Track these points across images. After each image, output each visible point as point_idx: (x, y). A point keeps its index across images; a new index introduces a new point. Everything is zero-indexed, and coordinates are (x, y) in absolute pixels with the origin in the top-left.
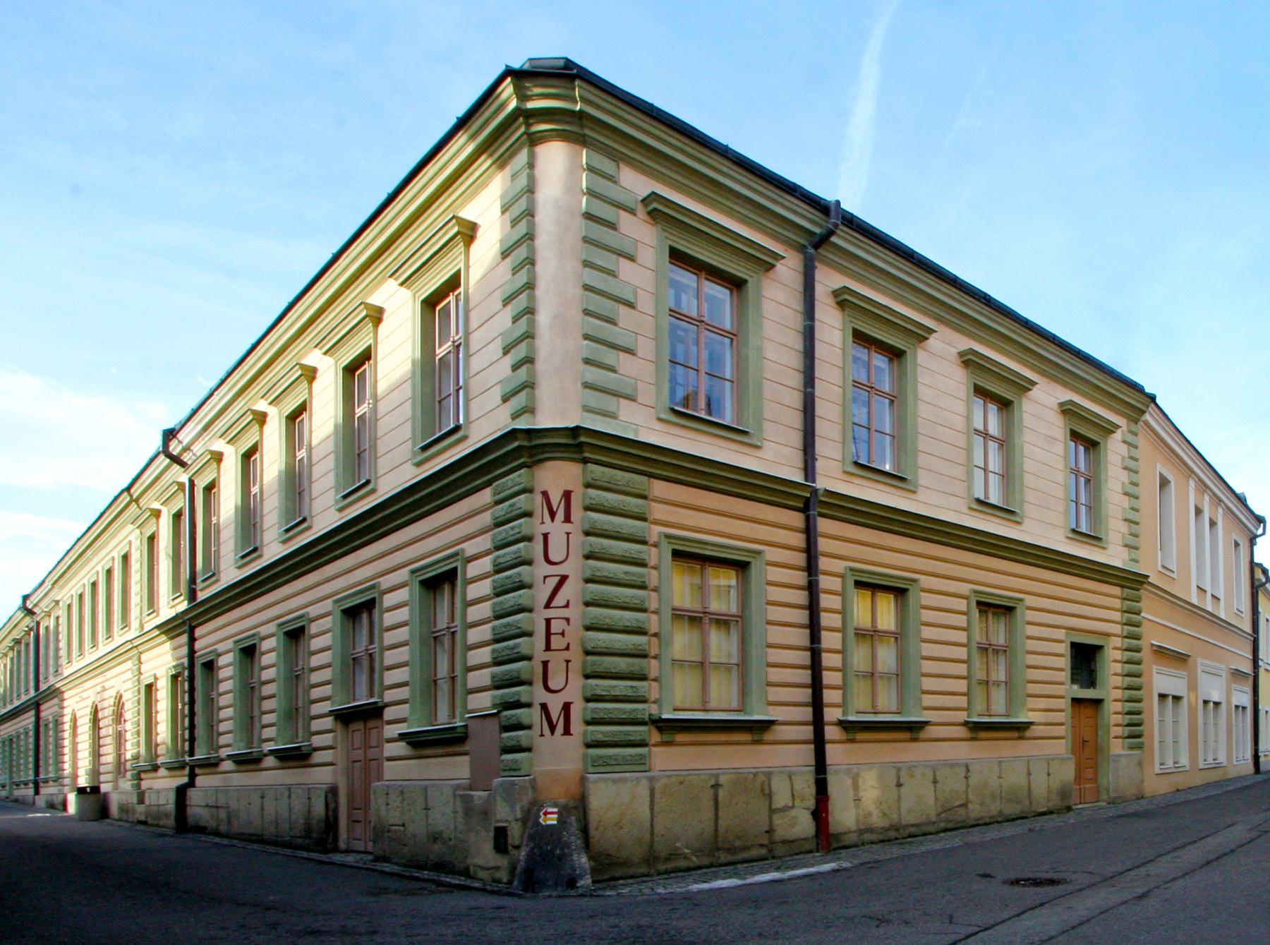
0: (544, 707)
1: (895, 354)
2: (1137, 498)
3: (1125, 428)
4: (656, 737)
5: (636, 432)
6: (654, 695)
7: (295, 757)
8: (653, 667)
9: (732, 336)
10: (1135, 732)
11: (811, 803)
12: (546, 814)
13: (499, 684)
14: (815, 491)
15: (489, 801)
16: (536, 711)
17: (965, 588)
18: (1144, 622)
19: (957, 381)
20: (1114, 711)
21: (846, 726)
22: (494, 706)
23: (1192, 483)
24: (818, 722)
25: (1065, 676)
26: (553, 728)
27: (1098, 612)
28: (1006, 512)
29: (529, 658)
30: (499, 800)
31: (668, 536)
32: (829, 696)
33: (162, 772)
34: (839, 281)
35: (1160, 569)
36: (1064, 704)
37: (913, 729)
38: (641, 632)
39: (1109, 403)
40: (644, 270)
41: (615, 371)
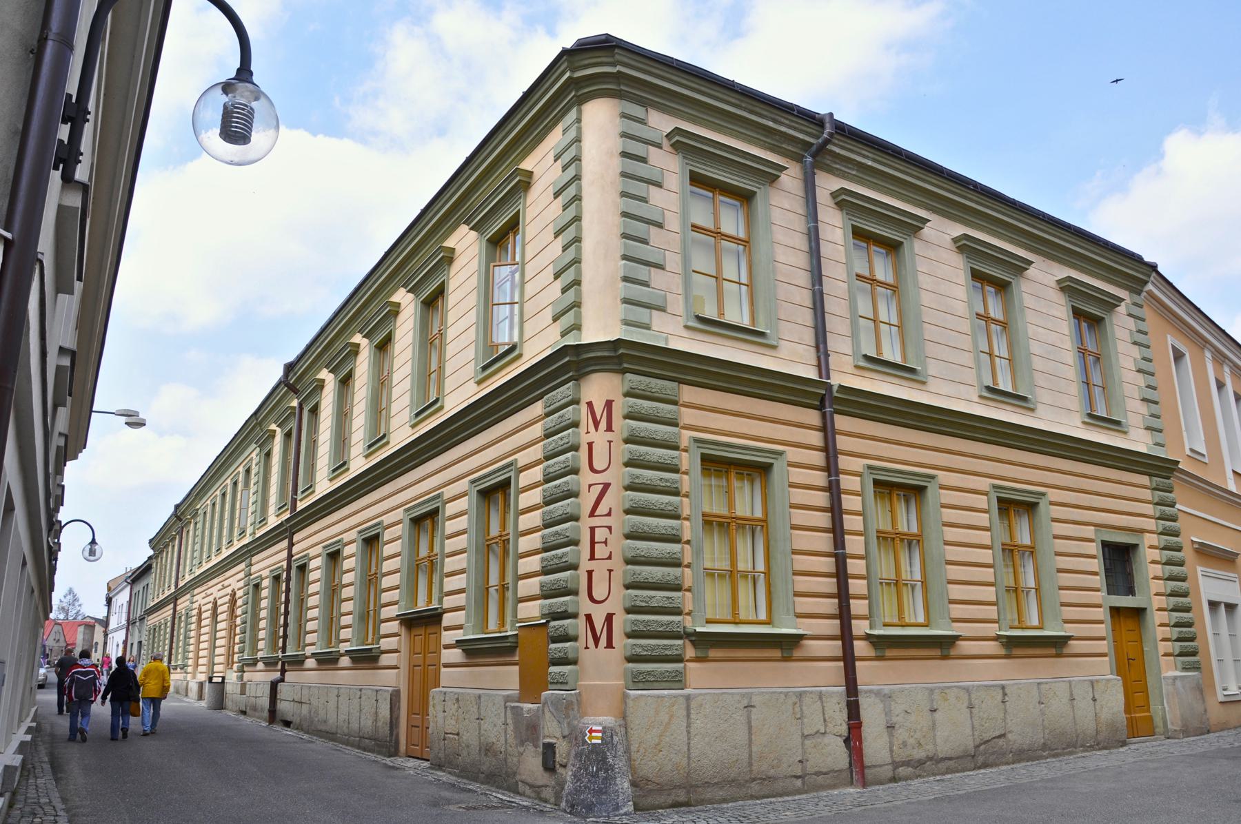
0: (589, 618)
1: (893, 247)
2: (1152, 374)
3: (1128, 301)
4: (690, 652)
5: (667, 340)
6: (688, 606)
8: (688, 576)
9: (745, 243)
10: (1189, 649)
11: (844, 729)
13: (548, 593)
14: (829, 387)
16: (582, 621)
17: (984, 484)
18: (1180, 515)
19: (956, 269)
20: (1158, 621)
21: (880, 643)
22: (543, 616)
23: (1208, 355)
24: (846, 636)
25: (1099, 581)
26: (596, 640)
27: (1129, 506)
28: (1018, 400)
30: (548, 714)
31: (696, 440)
32: (858, 607)
34: (836, 184)
35: (1188, 452)
36: (1101, 614)
37: (943, 646)
39: (1107, 278)
40: (670, 195)
41: (648, 286)
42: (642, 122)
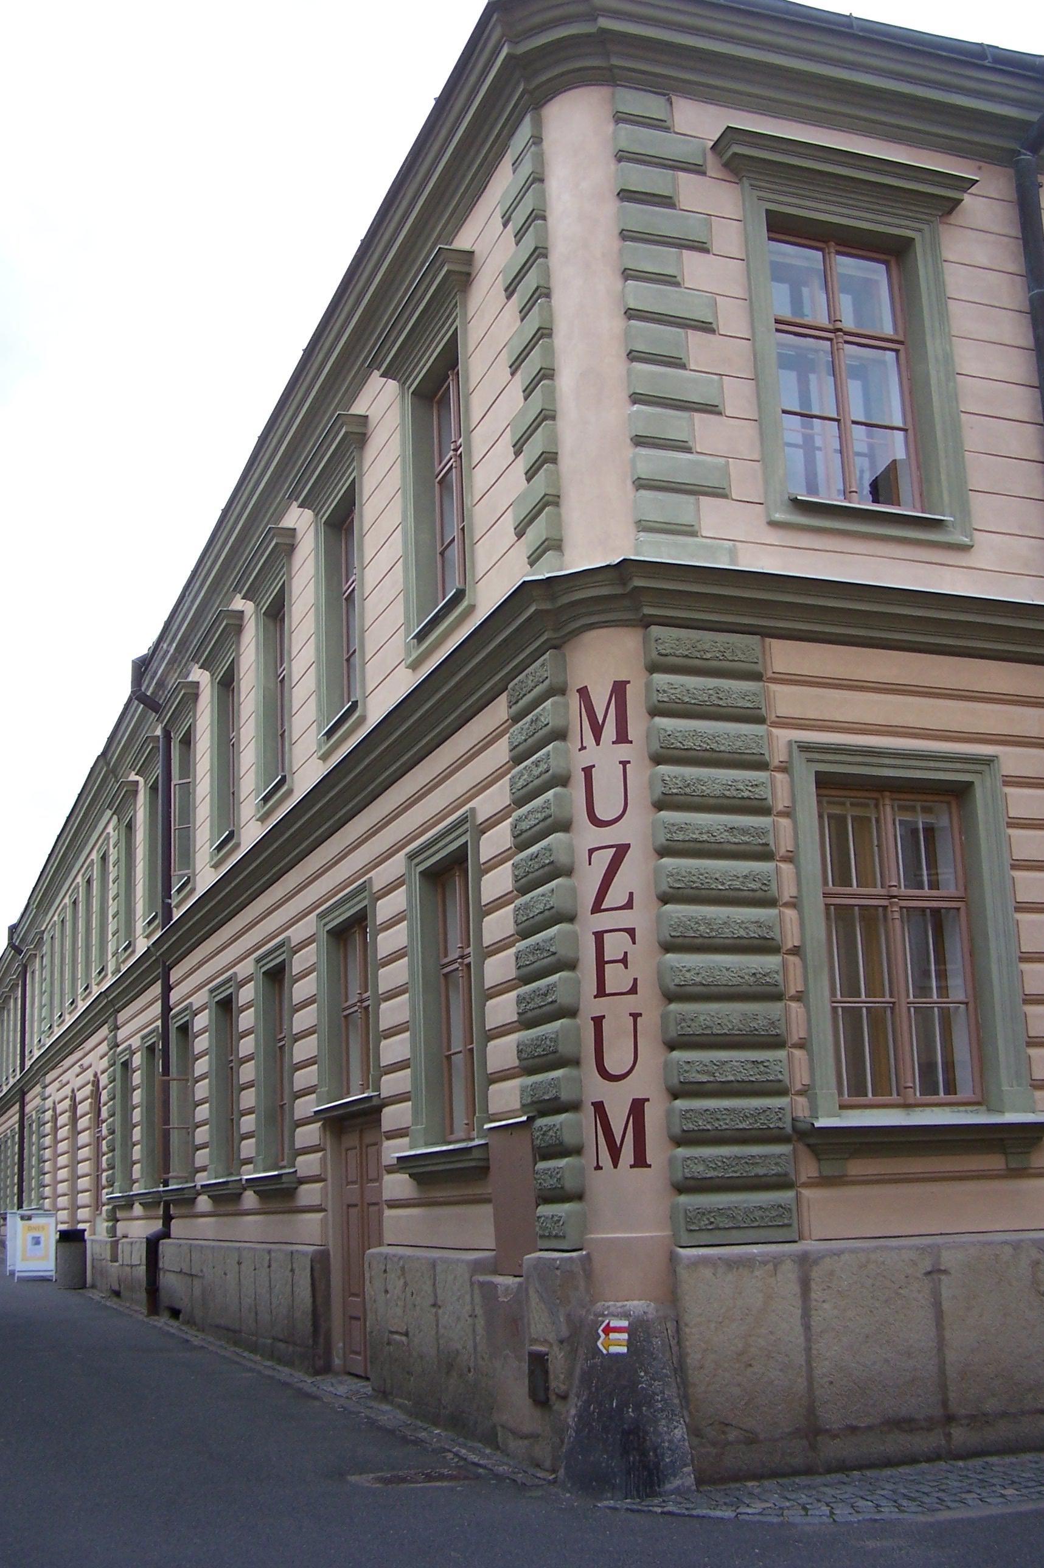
0: (599, 1108)
5: (733, 554)
7: (278, 1194)
12: (608, 1330)
15: (520, 1297)
26: (615, 1153)
29: (572, 1013)
31: (805, 748)
33: (138, 1210)
38: (765, 946)
40: (726, 266)
41: (689, 450)
42: (660, 125)
